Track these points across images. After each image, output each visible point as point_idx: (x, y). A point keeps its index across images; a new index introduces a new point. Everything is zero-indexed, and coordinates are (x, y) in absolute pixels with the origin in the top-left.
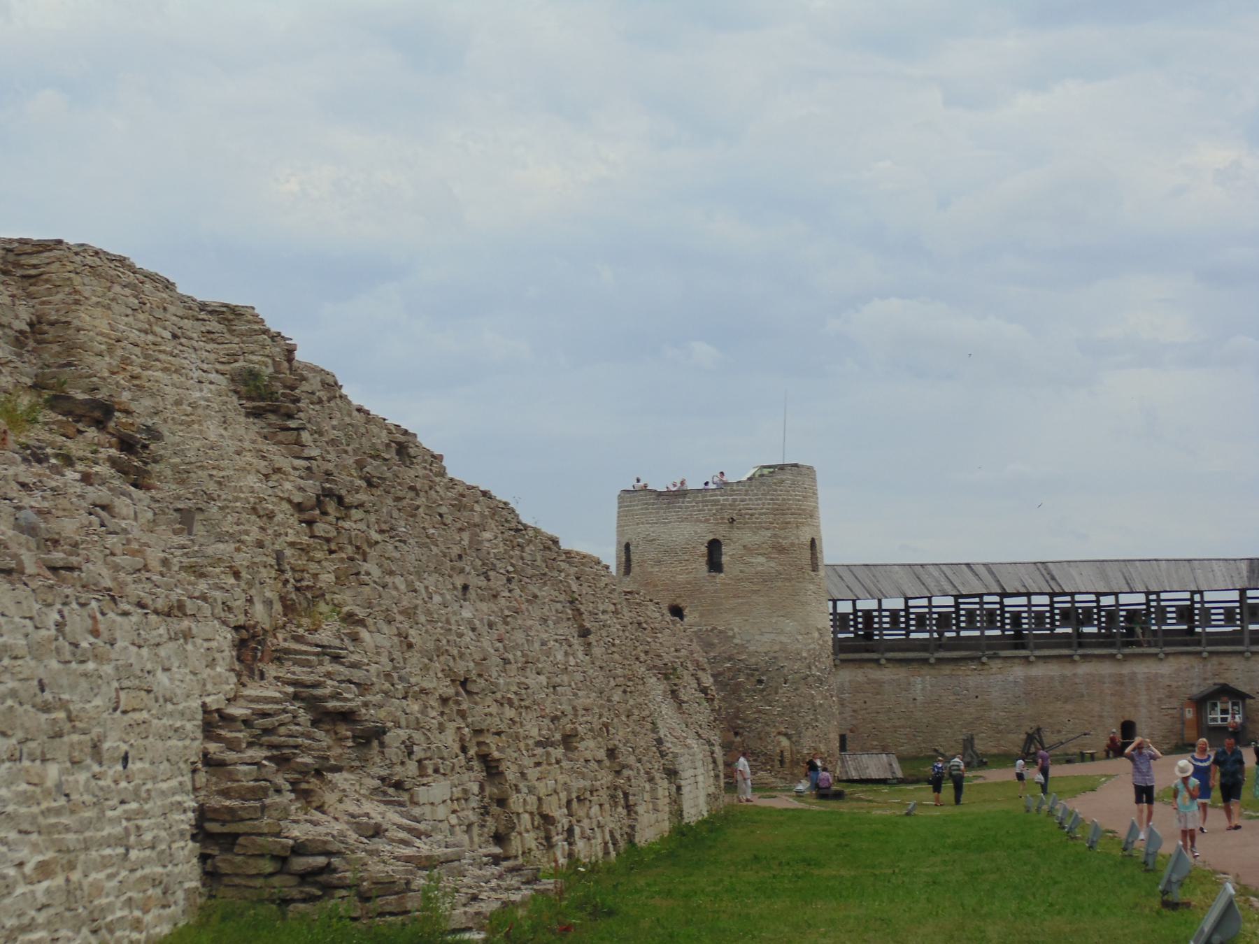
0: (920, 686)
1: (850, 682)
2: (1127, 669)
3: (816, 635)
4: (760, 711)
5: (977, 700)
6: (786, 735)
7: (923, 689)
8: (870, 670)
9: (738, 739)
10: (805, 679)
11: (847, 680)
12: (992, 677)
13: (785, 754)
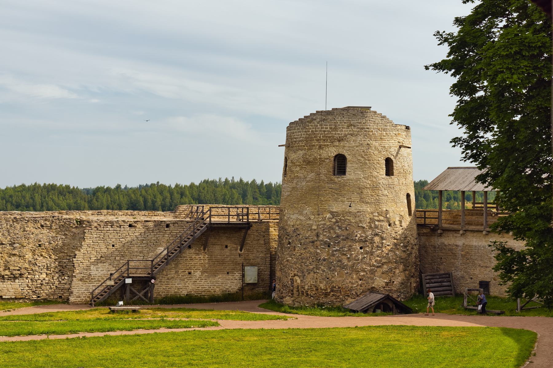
3: (328, 215)
4: (288, 261)
6: (298, 275)
10: (313, 242)
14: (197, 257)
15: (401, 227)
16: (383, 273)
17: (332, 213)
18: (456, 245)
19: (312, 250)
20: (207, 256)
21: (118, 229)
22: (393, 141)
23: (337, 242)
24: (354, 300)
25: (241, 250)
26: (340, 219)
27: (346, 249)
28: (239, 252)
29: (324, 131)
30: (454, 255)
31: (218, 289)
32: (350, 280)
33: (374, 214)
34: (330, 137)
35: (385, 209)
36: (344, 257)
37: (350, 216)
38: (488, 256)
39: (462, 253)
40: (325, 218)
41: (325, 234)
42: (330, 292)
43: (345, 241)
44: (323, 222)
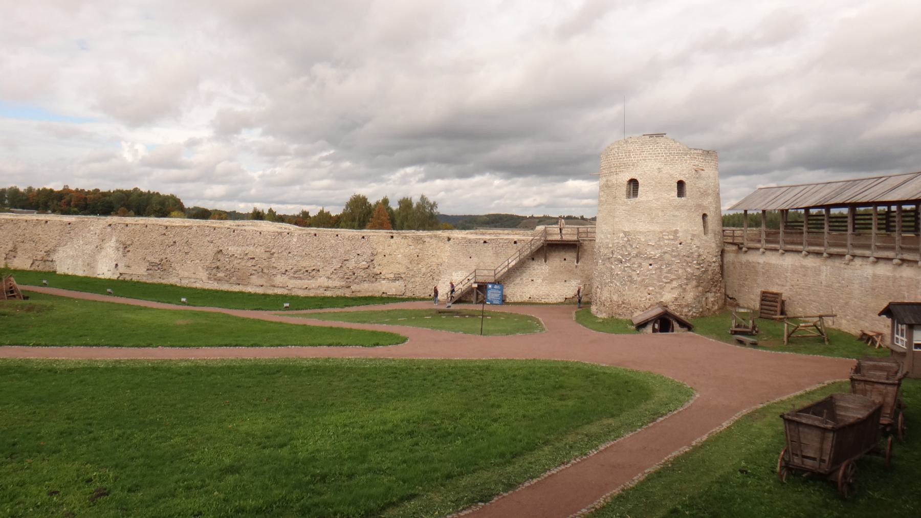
0: (824, 274)
1: (792, 265)
3: (622, 235)
7: (826, 276)
8: (802, 259)
10: (609, 259)
14: (539, 267)
15: (695, 246)
16: (672, 289)
17: (624, 232)
18: (759, 263)
19: (609, 265)
20: (548, 267)
21: (474, 244)
22: (687, 165)
23: (628, 259)
24: (643, 312)
25: (577, 262)
26: (632, 238)
27: (636, 266)
28: (576, 264)
29: (620, 159)
30: (757, 271)
31: (556, 294)
32: (639, 294)
33: (664, 234)
34: (624, 164)
35: (674, 229)
36: (634, 273)
37: (640, 236)
38: (784, 275)
39: (763, 270)
40: (619, 237)
41: (618, 251)
42: (621, 305)
43: (635, 259)
44: (616, 241)
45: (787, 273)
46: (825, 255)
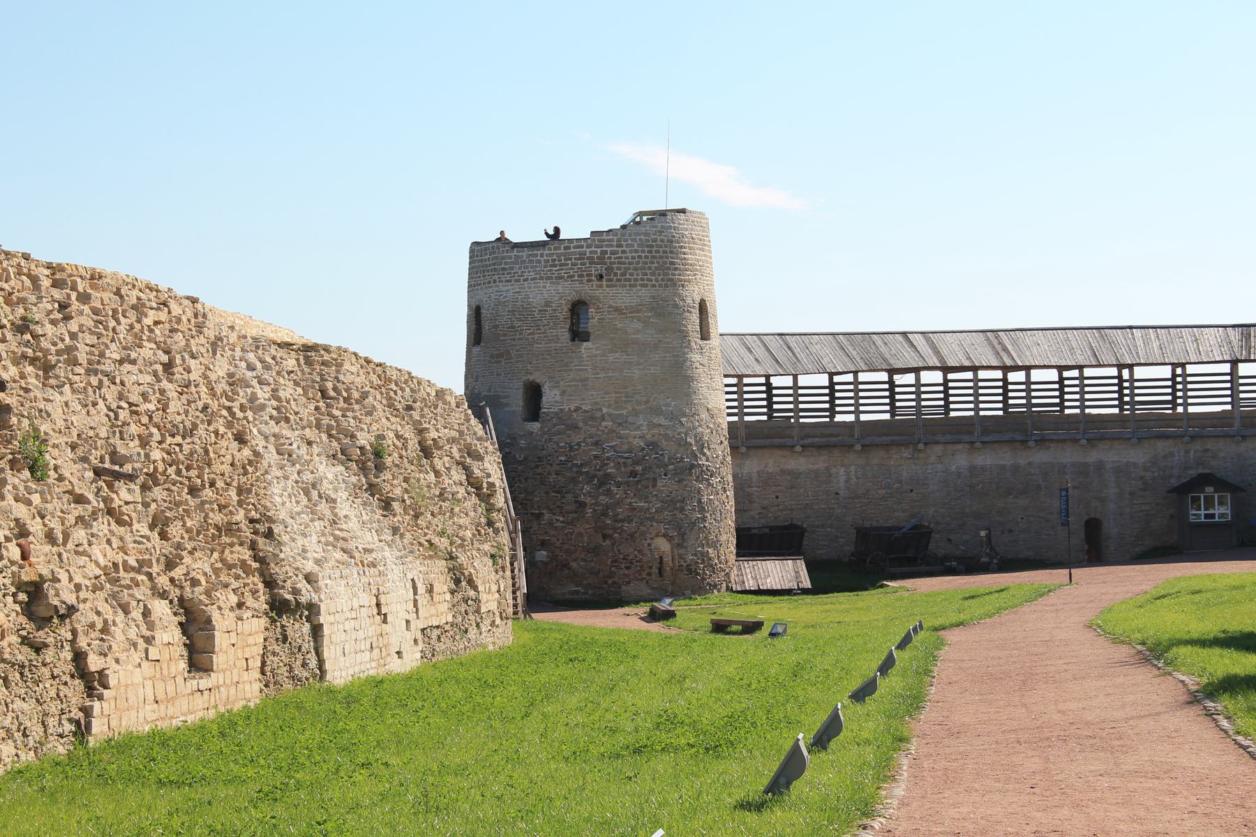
0: (843, 479)
1: (758, 472)
2: (1093, 456)
5: (912, 494)
6: (664, 536)
7: (847, 482)
9: (608, 542)
11: (755, 470)
12: (930, 467)
13: (665, 559)
45: (750, 487)
46: (858, 447)
